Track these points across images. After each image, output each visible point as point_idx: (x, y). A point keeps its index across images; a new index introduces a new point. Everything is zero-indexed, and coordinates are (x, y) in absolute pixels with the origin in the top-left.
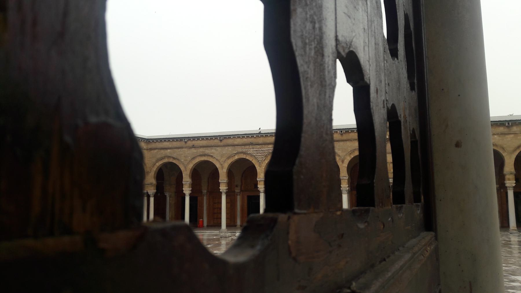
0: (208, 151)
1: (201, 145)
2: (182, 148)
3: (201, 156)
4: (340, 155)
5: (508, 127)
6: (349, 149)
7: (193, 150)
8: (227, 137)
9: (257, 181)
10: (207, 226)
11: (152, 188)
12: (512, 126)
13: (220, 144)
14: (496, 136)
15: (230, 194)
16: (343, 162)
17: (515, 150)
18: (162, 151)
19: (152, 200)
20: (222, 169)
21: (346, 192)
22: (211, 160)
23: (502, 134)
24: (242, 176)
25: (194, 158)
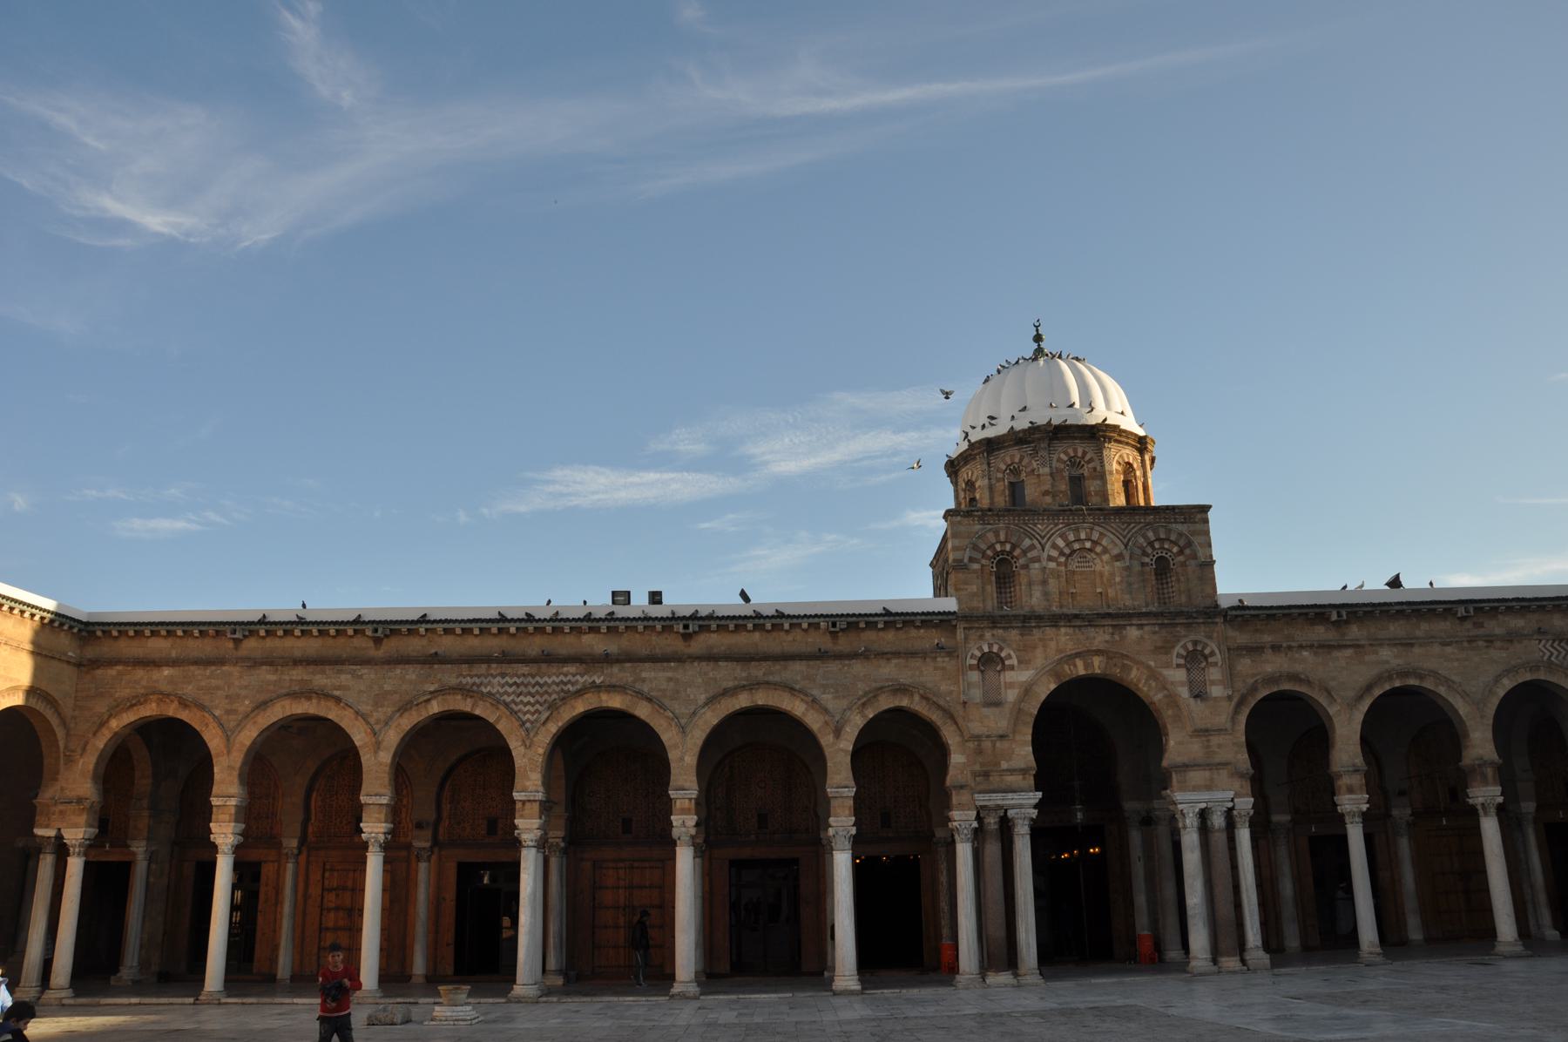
0: (321, 680)
1: (298, 654)
2: (219, 661)
3: (293, 695)
4: (830, 706)
5: (1338, 624)
6: (861, 687)
7: (266, 675)
8: (404, 628)
9: (514, 802)
10: (293, 978)
11: (83, 819)
12: (1347, 622)
13: (373, 653)
14: (1305, 653)
15: (394, 849)
16: (838, 732)
17: (1360, 698)
18: (140, 673)
19: (75, 866)
20: (376, 752)
21: (848, 845)
22: (332, 713)
23: (1321, 646)
24: (442, 786)
25: (262, 706)
